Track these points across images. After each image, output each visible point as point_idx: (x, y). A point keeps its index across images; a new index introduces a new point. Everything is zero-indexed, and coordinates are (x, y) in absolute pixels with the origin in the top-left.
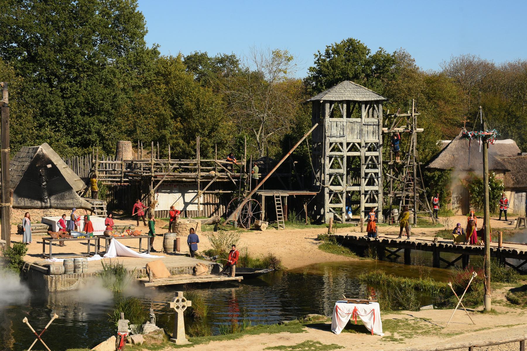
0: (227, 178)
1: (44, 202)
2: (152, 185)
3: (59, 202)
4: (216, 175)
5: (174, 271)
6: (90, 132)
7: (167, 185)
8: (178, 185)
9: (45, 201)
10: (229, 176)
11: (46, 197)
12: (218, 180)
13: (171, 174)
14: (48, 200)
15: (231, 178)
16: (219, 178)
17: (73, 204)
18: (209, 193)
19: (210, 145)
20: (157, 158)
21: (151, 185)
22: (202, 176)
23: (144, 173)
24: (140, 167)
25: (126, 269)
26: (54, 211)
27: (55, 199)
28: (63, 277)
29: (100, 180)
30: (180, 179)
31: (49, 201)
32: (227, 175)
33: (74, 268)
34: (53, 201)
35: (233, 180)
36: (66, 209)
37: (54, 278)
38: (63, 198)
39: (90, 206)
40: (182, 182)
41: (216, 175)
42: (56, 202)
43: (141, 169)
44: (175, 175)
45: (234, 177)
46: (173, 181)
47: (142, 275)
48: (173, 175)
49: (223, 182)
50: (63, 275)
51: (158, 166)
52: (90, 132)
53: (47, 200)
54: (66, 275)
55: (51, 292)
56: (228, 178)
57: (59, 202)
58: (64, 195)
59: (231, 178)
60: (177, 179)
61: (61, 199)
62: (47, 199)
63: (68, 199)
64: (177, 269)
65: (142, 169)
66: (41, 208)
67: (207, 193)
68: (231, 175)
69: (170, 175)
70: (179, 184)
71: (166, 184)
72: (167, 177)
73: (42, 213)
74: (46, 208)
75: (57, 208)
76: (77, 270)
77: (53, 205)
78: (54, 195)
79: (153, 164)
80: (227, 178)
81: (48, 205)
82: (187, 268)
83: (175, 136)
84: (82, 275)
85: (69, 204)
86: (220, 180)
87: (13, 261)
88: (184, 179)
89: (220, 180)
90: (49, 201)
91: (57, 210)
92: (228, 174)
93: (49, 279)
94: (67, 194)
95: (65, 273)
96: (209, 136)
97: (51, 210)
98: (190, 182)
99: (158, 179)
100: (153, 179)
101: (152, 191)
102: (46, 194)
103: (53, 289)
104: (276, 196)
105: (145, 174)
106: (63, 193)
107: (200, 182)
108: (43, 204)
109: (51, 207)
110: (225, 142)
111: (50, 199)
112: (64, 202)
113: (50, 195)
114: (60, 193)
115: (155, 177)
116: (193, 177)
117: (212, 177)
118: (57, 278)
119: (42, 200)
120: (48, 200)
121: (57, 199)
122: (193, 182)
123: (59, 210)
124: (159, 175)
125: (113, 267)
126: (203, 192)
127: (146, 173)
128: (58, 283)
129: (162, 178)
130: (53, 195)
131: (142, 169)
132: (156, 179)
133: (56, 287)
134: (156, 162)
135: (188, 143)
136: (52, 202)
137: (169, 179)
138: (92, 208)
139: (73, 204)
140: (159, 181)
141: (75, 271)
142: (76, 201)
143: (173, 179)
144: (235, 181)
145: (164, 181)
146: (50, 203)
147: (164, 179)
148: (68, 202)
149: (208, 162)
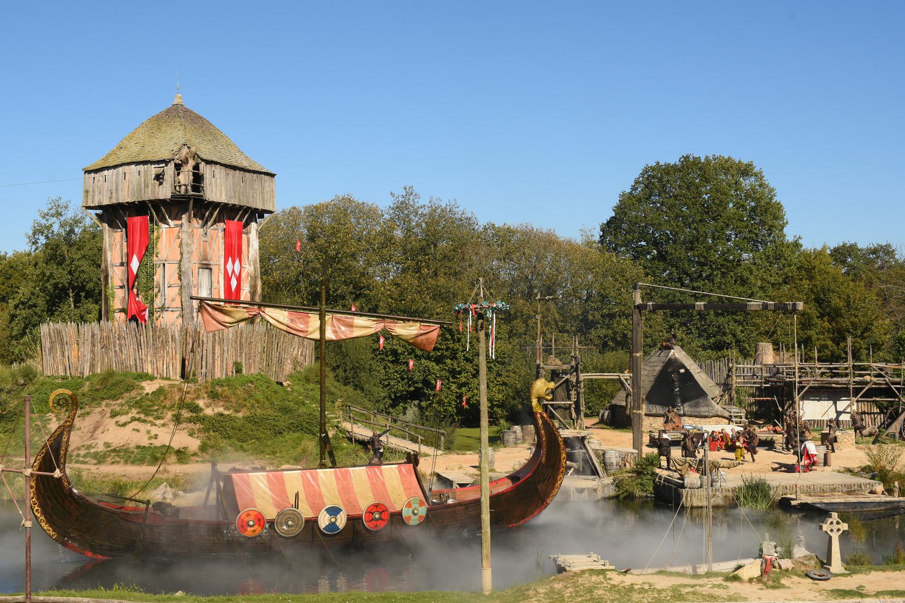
0: (884, 384)
3: (692, 410)
4: (871, 381)
6: (724, 334)
7: (813, 392)
10: (888, 381)
12: (874, 386)
14: (681, 407)
15: (890, 384)
16: (875, 384)
18: (864, 401)
19: (864, 347)
20: (801, 361)
22: (854, 382)
24: (783, 372)
27: (689, 406)
28: (699, 492)
29: (738, 385)
30: (829, 385)
32: (885, 381)
34: (686, 408)
35: (892, 386)
37: (690, 492)
39: (727, 414)
40: (832, 388)
41: (871, 381)
43: (783, 374)
45: (894, 383)
46: (821, 388)
47: (788, 491)
49: (880, 388)
51: (803, 371)
52: (724, 334)
54: (702, 489)
55: (686, 507)
56: (887, 384)
57: (692, 410)
58: (698, 402)
59: (890, 384)
60: (826, 385)
61: (695, 406)
62: (680, 406)
64: (828, 486)
65: (785, 373)
67: (861, 401)
68: (889, 380)
69: (817, 381)
75: (690, 416)
76: (714, 484)
79: (797, 368)
80: (884, 384)
83: (821, 337)
86: (876, 386)
87: (646, 473)
88: (834, 385)
89: (876, 386)
91: (691, 418)
92: (886, 379)
93: (684, 493)
95: (701, 486)
96: (862, 337)
98: (841, 388)
101: (797, 398)
102: (679, 400)
105: (788, 379)
107: (853, 388)
109: (684, 415)
110: (881, 343)
111: (683, 407)
112: (698, 410)
113: (683, 402)
116: (844, 382)
117: (867, 383)
120: (681, 407)
121: (691, 406)
122: (844, 388)
124: (805, 381)
125: (754, 483)
126: (856, 399)
127: (790, 378)
128: (693, 498)
131: (785, 373)
132: (801, 385)
134: (800, 366)
135: (838, 344)
136: (686, 409)
137: (816, 385)
140: (805, 387)
141: (712, 486)
143: (821, 385)
144: (895, 388)
145: (811, 387)
147: (811, 385)
148: (703, 410)
149: (862, 365)
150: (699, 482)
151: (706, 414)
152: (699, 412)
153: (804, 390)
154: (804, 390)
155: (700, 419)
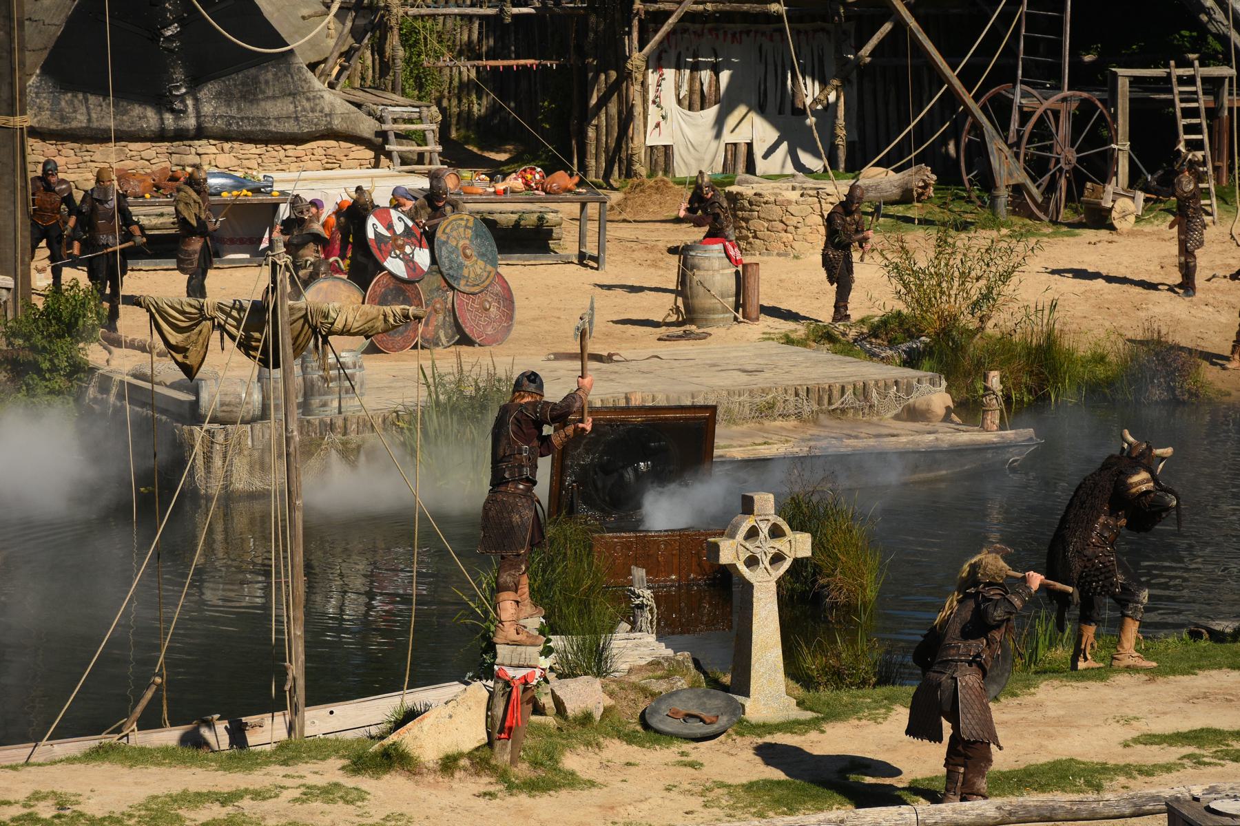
1: (173, 111)
2: (635, 35)
3: (233, 112)
5: (736, 408)
8: (748, 33)
9: (178, 105)
11: (178, 88)
14: (190, 102)
17: (297, 119)
21: (630, 33)
26: (213, 149)
27: (218, 96)
31: (190, 109)
33: (305, 395)
36: (266, 142)
37: (220, 438)
38: (250, 94)
39: (367, 127)
42: (222, 110)
50: (258, 426)
53: (183, 101)
57: (233, 112)
58: (256, 81)
61: (243, 98)
62: (182, 98)
63: (274, 98)
64: (745, 398)
66: (161, 136)
71: (698, 26)
73: (163, 158)
74: (180, 135)
75: (225, 137)
76: (316, 401)
77: (209, 124)
78: (214, 78)
81: (191, 122)
84: (340, 422)
85: (277, 119)
87: (46, 365)
90: (190, 109)
91: (227, 146)
94: (270, 76)
95: (264, 415)
97: (203, 146)
101: (637, 59)
102: (179, 75)
103: (216, 488)
106: (253, 71)
108: (169, 119)
109: (201, 133)
111: (196, 100)
112: (256, 111)
113: (195, 82)
114: (237, 72)
118: (233, 440)
119: (162, 102)
120: (190, 102)
121: (226, 97)
123: (236, 145)
125: (469, 391)
128: (236, 461)
130: (208, 80)
133: (228, 476)
136: (207, 109)
138: (378, 134)
139: (297, 119)
140: (668, 14)
141: (305, 407)
142: (307, 105)
145: (689, 17)
146: (198, 116)
150: (257, 397)
151: (289, 127)
152: (260, 121)
153: (665, 28)
154: (665, 28)
155: (261, 149)
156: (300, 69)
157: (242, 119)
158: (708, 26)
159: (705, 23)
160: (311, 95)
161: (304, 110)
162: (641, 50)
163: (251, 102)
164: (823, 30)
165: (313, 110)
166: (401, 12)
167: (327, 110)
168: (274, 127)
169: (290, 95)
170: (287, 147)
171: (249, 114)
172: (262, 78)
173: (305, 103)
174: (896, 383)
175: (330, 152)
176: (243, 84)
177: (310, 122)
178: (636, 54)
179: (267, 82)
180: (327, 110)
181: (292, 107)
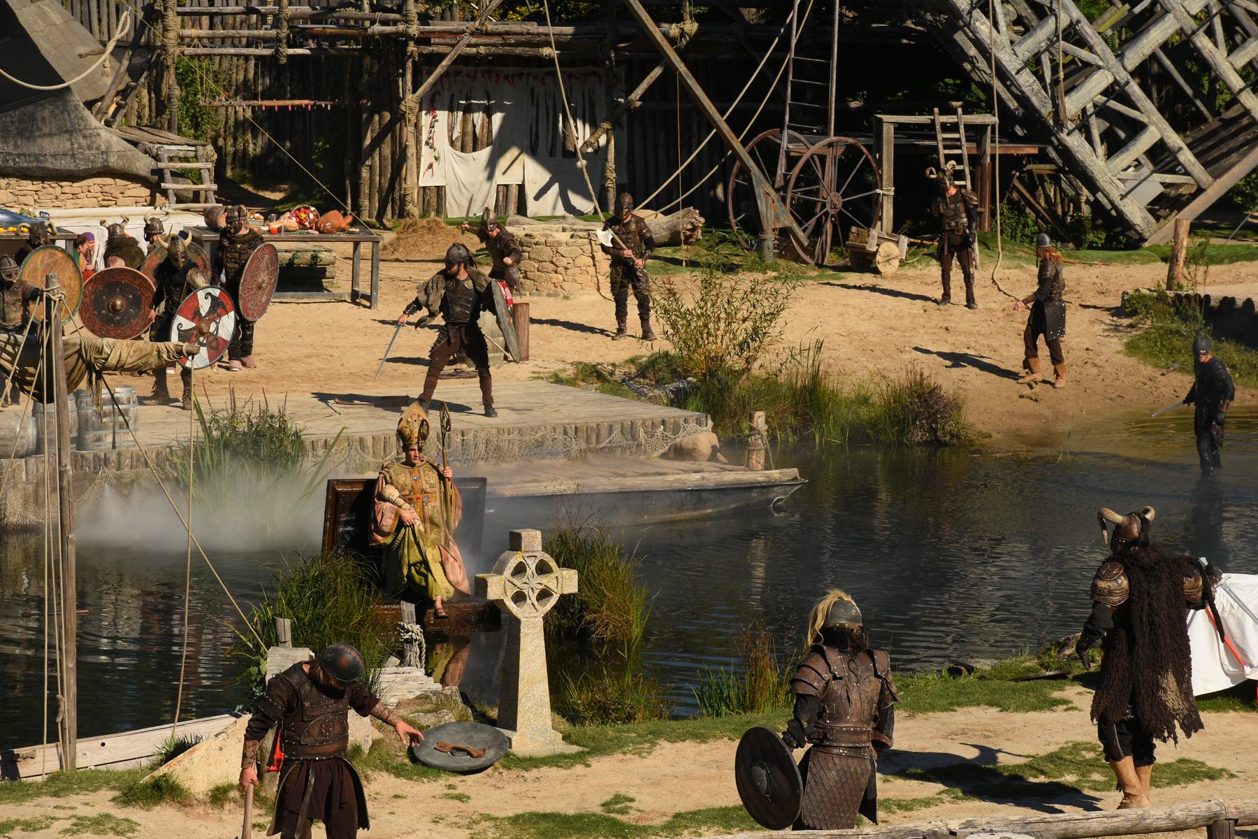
2: (409, 77)
8: (520, 76)
13: (490, 27)
17: (73, 156)
21: (403, 75)
23: (373, 23)
25: (297, 434)
29: (189, 51)
30: (529, 51)
33: (79, 430)
36: (43, 179)
38: (27, 131)
39: (143, 165)
44: (508, 33)
47: (370, 458)
48: (500, 34)
50: (32, 460)
57: (10, 148)
58: (33, 118)
60: (518, 50)
63: (50, 135)
64: (515, 435)
70: (525, 71)
72: (473, 40)
76: (90, 436)
82: (560, 430)
84: (113, 457)
85: (54, 156)
94: (46, 113)
95: (38, 449)
99: (435, 48)
100: (412, 47)
101: (410, 100)
104: (943, 125)
105: (377, 28)
106: (30, 108)
112: (33, 148)
114: (14, 108)
115: (423, 40)
123: (13, 181)
124: (442, 34)
125: (242, 427)
127: (385, 23)
129: (453, 46)
132: (427, 50)
137: (482, 50)
138: (154, 172)
139: (73, 156)
140: (442, 57)
142: (84, 142)
143: (500, 50)
145: (463, 60)
147: (462, 49)
148: (52, 148)
150: (31, 431)
151: (65, 164)
152: (36, 157)
153: (439, 71)
154: (439, 71)
155: (38, 185)
156: (76, 107)
157: (19, 155)
158: (480, 68)
159: (478, 65)
160: (87, 133)
161: (80, 147)
162: (414, 91)
163: (28, 139)
164: (594, 74)
165: (89, 148)
166: (177, 52)
167: (103, 148)
168: (50, 164)
169: (66, 132)
170: (64, 184)
171: (25, 150)
172: (39, 115)
173: (81, 140)
174: (663, 422)
175: (106, 189)
176: (20, 121)
177: (87, 159)
178: (409, 96)
179: (43, 119)
180: (103, 148)
181: (68, 144)
